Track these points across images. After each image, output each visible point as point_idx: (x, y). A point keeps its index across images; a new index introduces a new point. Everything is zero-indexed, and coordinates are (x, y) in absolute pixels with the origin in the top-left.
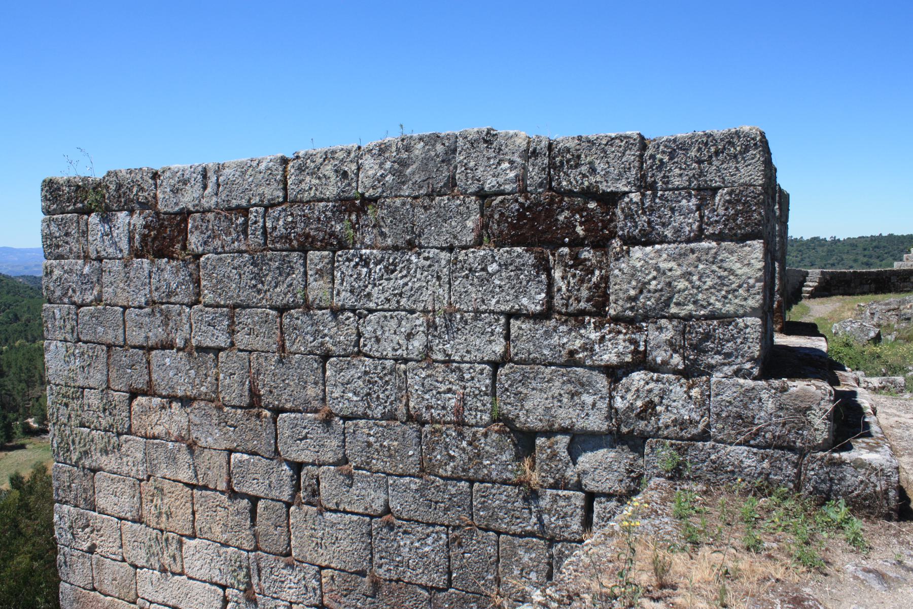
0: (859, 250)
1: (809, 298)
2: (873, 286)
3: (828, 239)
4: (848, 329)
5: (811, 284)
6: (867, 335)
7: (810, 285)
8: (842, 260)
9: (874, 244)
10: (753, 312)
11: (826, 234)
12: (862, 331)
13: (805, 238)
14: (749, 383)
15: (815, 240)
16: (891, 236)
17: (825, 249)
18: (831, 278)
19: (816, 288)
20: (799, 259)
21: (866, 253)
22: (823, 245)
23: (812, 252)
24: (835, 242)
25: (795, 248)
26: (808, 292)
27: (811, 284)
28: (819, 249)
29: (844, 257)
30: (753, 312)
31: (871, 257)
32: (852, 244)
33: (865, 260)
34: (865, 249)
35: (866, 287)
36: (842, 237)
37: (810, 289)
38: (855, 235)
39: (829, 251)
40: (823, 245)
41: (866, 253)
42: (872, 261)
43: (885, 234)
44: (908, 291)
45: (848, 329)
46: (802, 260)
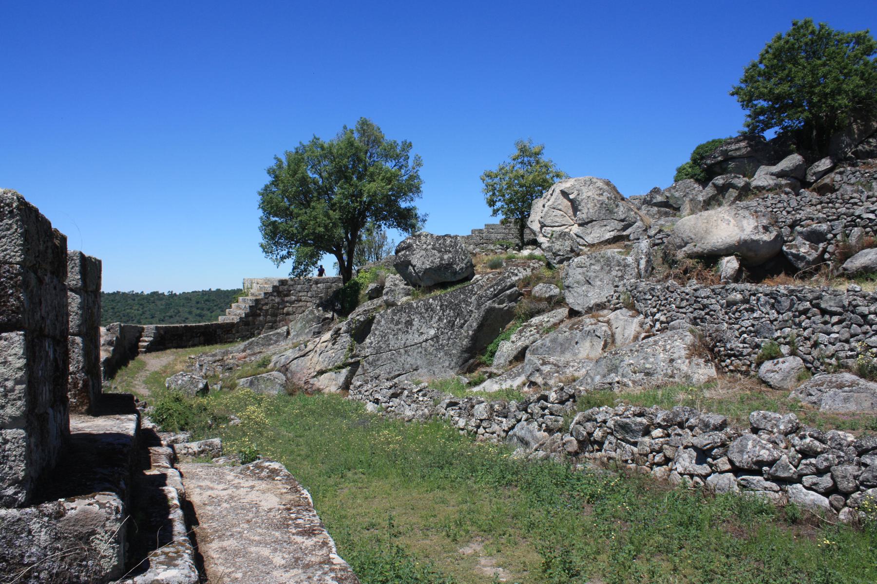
1: (146, 352)
2: (202, 338)
3: (166, 294)
4: (180, 382)
5: (146, 339)
6: (196, 386)
7: (146, 340)
9: (206, 298)
10: (14, 422)
11: (164, 290)
12: (192, 383)
13: (145, 293)
14: (13, 512)
15: (154, 294)
16: (218, 290)
18: (165, 333)
19: (151, 342)
20: (140, 312)
21: (199, 305)
23: (152, 306)
24: (172, 296)
25: (136, 302)
26: (144, 347)
27: (146, 339)
28: (158, 303)
29: (181, 309)
30: (14, 422)
31: (203, 309)
32: (187, 298)
33: (198, 312)
34: (198, 303)
35: (196, 340)
36: (178, 291)
37: (146, 344)
38: (189, 290)
39: (167, 304)
41: (199, 305)
42: (204, 312)
43: (214, 289)
44: (231, 342)
45: (180, 382)
46: (143, 313)
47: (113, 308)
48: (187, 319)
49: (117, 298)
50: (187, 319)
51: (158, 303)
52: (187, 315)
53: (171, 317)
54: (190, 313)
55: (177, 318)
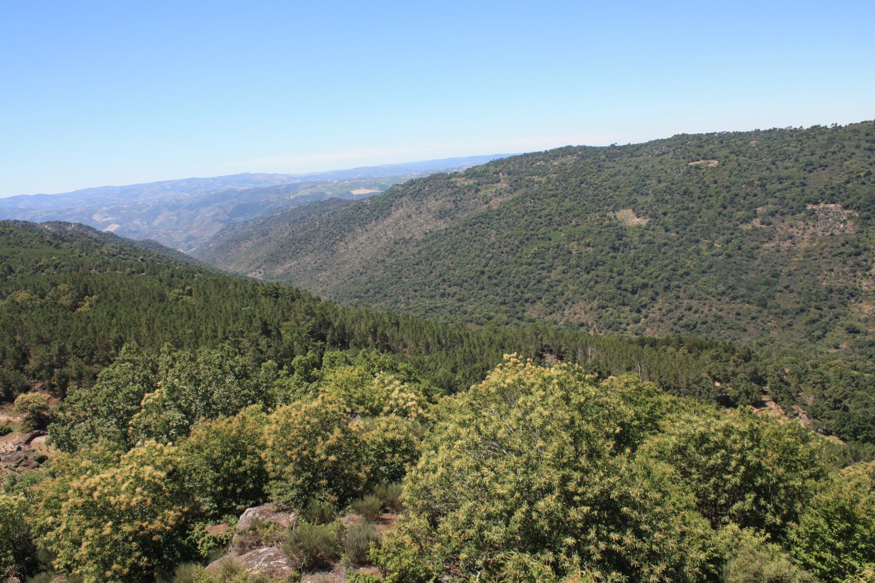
0: (862, 135)
3: (829, 127)
8: (844, 147)
11: (827, 122)
13: (805, 128)
17: (826, 137)
20: (798, 149)
21: (869, 138)
22: (824, 133)
24: (836, 128)
25: (794, 138)
28: (820, 138)
29: (846, 144)
33: (868, 145)
34: (868, 135)
36: (843, 123)
39: (830, 139)
40: (824, 133)
46: (802, 150)
47: (769, 147)
48: (853, 154)
49: (774, 135)
50: (853, 154)
51: (820, 138)
52: (854, 150)
53: (834, 153)
54: (858, 147)
55: (841, 153)
